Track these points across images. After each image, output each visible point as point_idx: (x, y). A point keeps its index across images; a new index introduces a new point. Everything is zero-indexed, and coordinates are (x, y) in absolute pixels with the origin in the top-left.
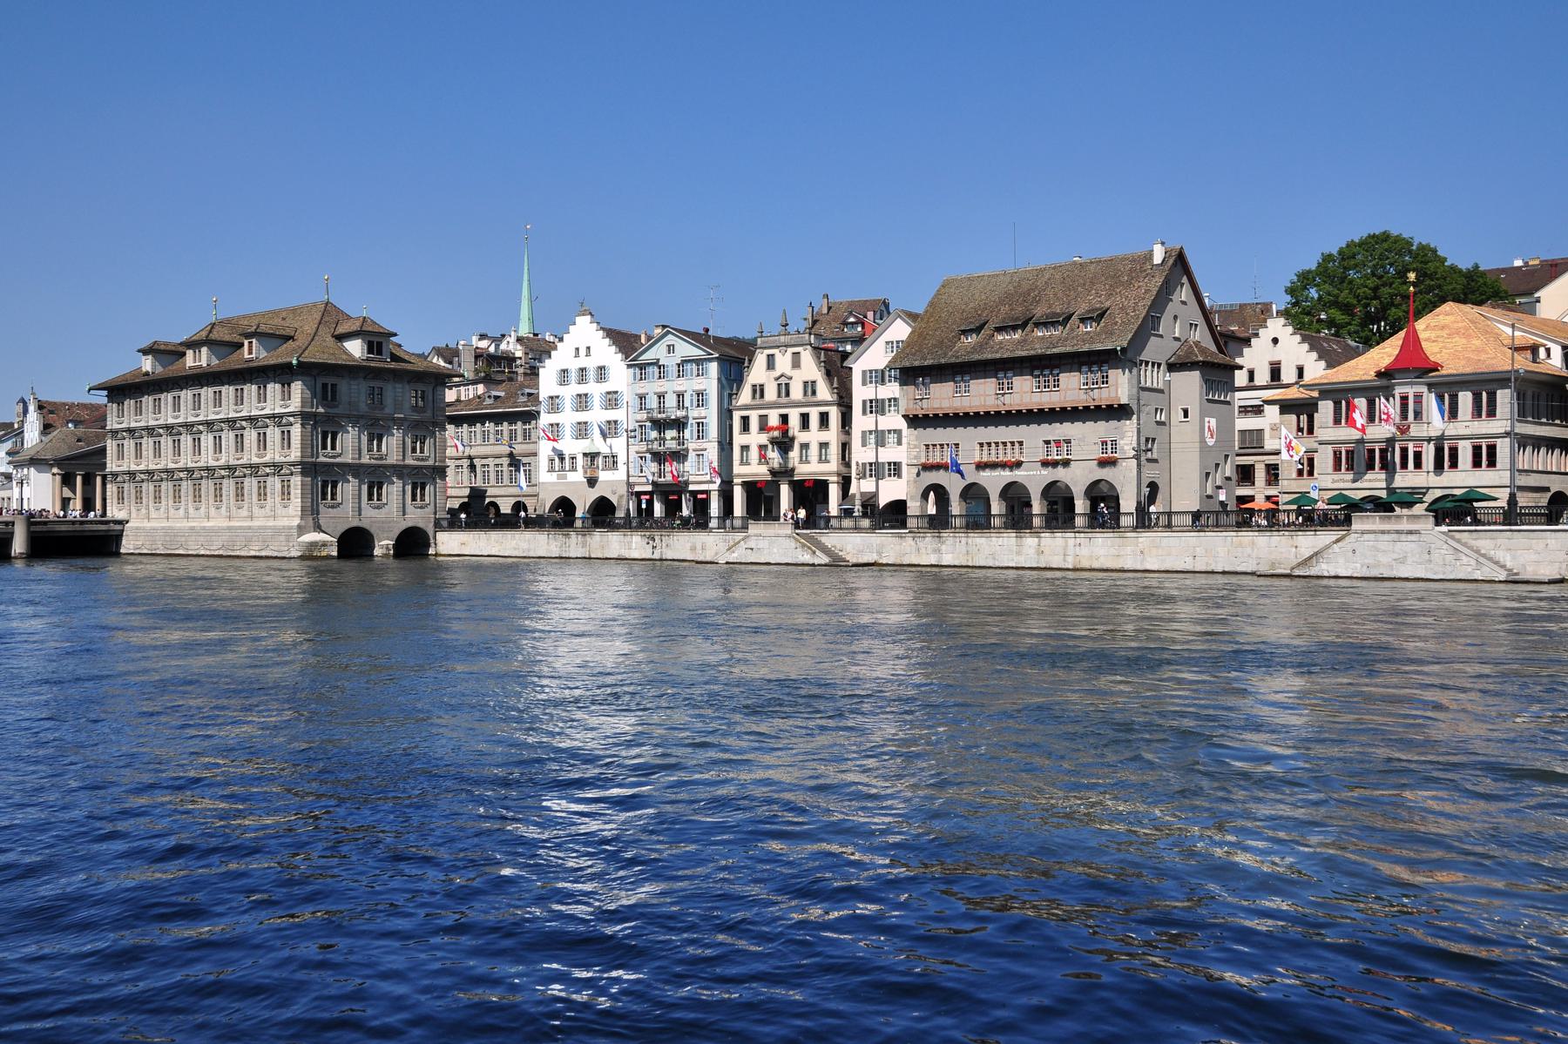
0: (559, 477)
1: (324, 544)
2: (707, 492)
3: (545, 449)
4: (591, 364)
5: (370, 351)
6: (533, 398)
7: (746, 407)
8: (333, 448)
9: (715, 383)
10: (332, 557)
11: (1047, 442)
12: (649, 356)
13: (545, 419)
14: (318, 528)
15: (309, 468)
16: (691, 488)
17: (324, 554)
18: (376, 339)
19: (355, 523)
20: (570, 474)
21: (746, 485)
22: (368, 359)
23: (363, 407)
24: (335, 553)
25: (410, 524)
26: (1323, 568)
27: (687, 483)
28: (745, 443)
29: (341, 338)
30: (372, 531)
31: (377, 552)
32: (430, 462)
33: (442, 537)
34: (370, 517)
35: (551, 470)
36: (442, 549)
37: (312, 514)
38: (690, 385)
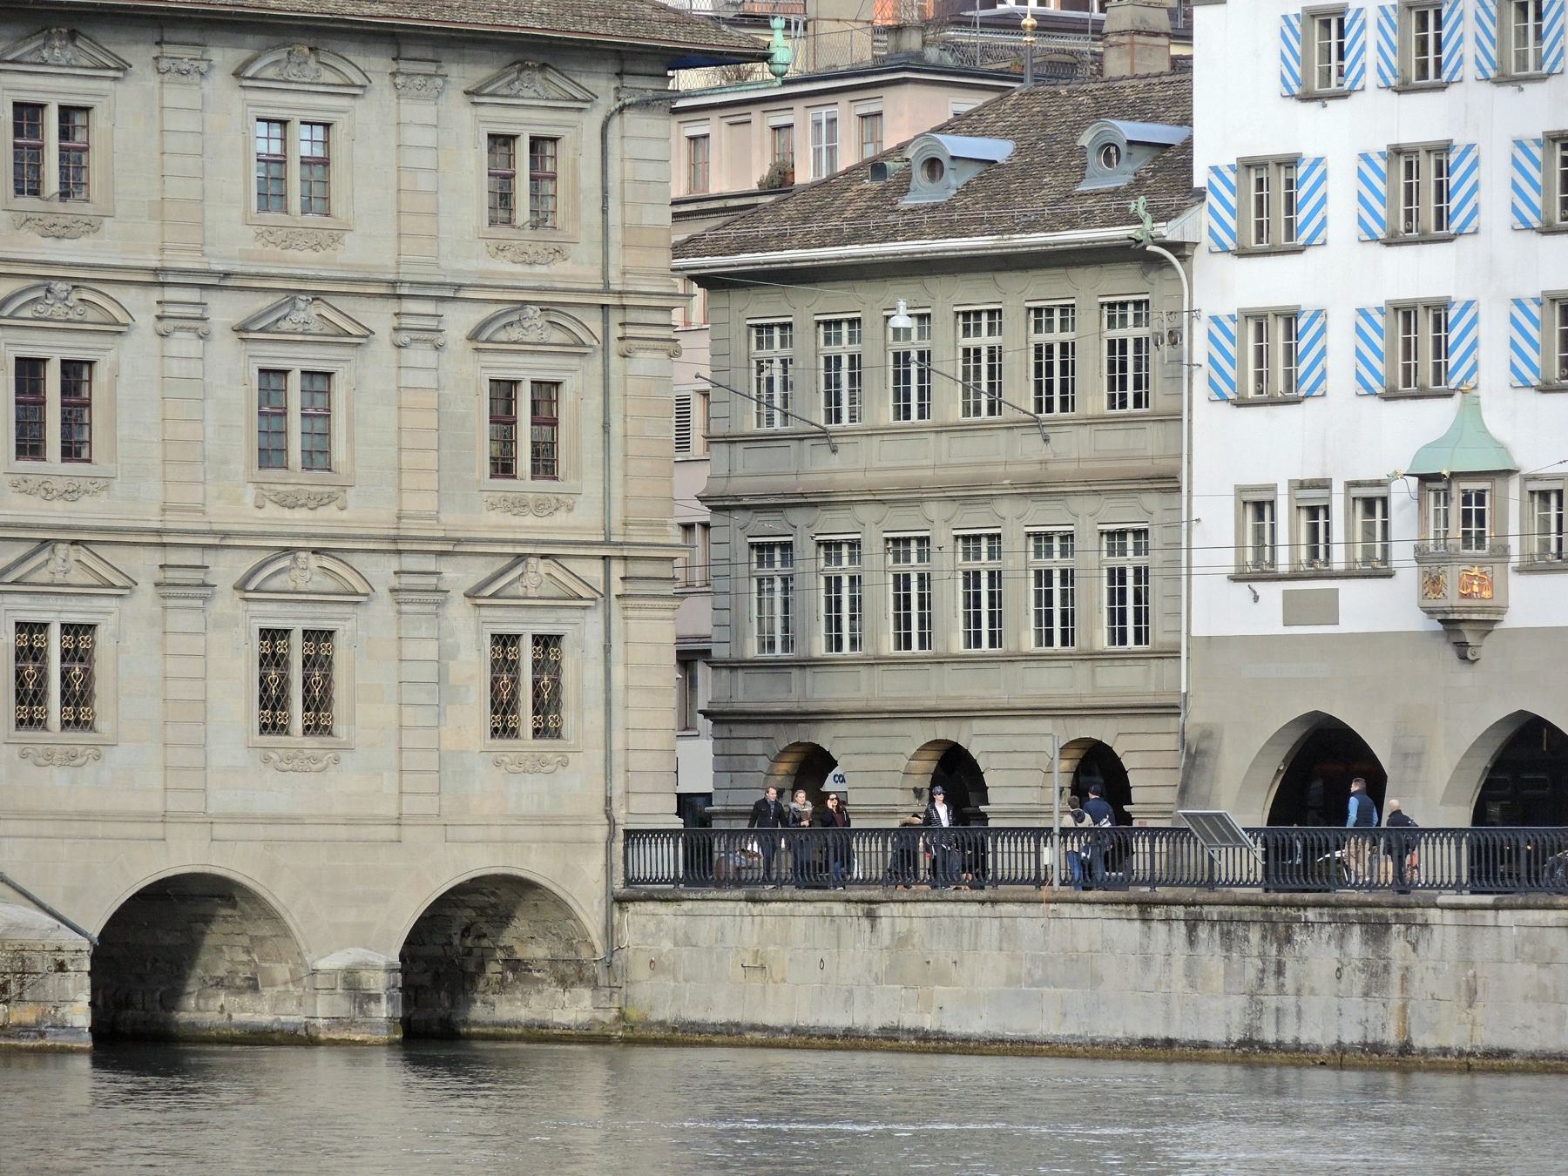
0: (1294, 610)
3: (1231, 450)
6: (1170, 171)
13: (1224, 287)
20: (1349, 591)
23: (232, 234)
33: (651, 928)
35: (1255, 572)
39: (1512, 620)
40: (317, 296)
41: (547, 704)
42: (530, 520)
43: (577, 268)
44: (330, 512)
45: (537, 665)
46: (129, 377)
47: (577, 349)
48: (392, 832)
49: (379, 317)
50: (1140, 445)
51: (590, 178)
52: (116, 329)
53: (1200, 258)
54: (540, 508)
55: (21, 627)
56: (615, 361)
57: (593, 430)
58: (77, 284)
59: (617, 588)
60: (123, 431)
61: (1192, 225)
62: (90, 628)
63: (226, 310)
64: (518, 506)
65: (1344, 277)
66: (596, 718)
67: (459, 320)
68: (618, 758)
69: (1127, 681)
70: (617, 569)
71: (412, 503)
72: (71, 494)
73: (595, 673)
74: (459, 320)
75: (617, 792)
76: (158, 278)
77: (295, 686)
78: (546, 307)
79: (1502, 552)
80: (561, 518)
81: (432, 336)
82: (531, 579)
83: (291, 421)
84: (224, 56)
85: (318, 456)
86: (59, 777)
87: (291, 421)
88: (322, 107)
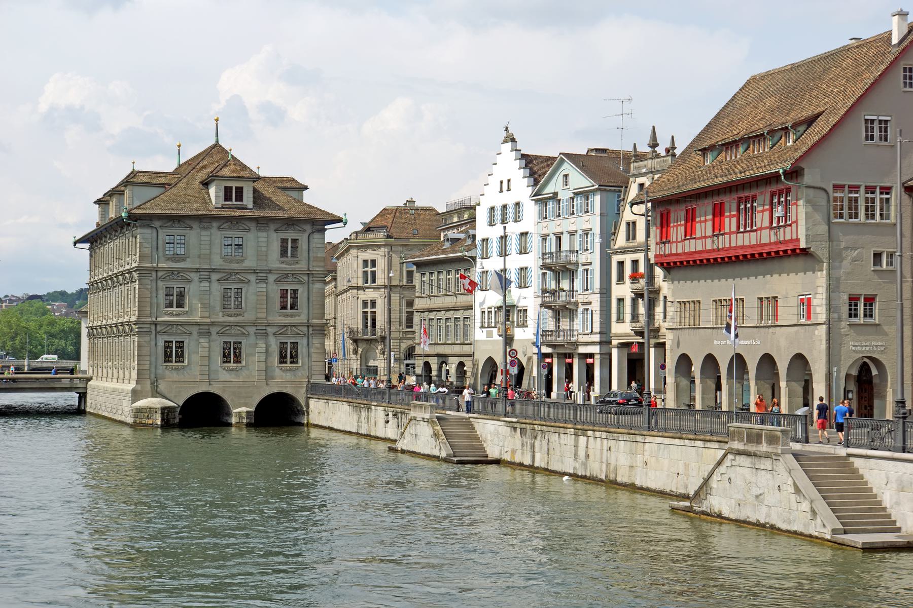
1: (150, 411)
2: (591, 355)
4: (509, 199)
5: (228, 197)
7: (622, 251)
8: (180, 305)
9: (598, 219)
10: (153, 426)
11: (761, 299)
12: (549, 190)
14: (156, 393)
15: (145, 328)
16: (582, 350)
17: (150, 422)
18: (234, 185)
19: (204, 388)
21: (622, 346)
24: (159, 423)
25: (275, 389)
26: (717, 502)
27: (576, 344)
28: (620, 296)
29: (206, 184)
30: (225, 396)
32: (303, 318)
34: (223, 382)
36: (314, 418)
37: (149, 382)
38: (579, 223)
39: (516, 338)
40: (237, 273)
43: (302, 265)
44: (241, 317)
46: (194, 290)
49: (252, 278)
50: (463, 300)
51: (305, 247)
52: (190, 281)
54: (292, 316)
55: (166, 342)
57: (305, 299)
59: (311, 332)
62: (183, 342)
63: (215, 277)
64: (286, 315)
65: (493, 264)
67: (272, 278)
69: (466, 349)
70: (311, 329)
71: (259, 315)
73: (305, 350)
74: (272, 278)
76: (198, 270)
77: (232, 354)
78: (293, 275)
79: (513, 322)
81: (265, 281)
82: (289, 331)
83: (232, 300)
84: (215, 224)
86: (175, 373)
87: (232, 300)
88: (240, 234)
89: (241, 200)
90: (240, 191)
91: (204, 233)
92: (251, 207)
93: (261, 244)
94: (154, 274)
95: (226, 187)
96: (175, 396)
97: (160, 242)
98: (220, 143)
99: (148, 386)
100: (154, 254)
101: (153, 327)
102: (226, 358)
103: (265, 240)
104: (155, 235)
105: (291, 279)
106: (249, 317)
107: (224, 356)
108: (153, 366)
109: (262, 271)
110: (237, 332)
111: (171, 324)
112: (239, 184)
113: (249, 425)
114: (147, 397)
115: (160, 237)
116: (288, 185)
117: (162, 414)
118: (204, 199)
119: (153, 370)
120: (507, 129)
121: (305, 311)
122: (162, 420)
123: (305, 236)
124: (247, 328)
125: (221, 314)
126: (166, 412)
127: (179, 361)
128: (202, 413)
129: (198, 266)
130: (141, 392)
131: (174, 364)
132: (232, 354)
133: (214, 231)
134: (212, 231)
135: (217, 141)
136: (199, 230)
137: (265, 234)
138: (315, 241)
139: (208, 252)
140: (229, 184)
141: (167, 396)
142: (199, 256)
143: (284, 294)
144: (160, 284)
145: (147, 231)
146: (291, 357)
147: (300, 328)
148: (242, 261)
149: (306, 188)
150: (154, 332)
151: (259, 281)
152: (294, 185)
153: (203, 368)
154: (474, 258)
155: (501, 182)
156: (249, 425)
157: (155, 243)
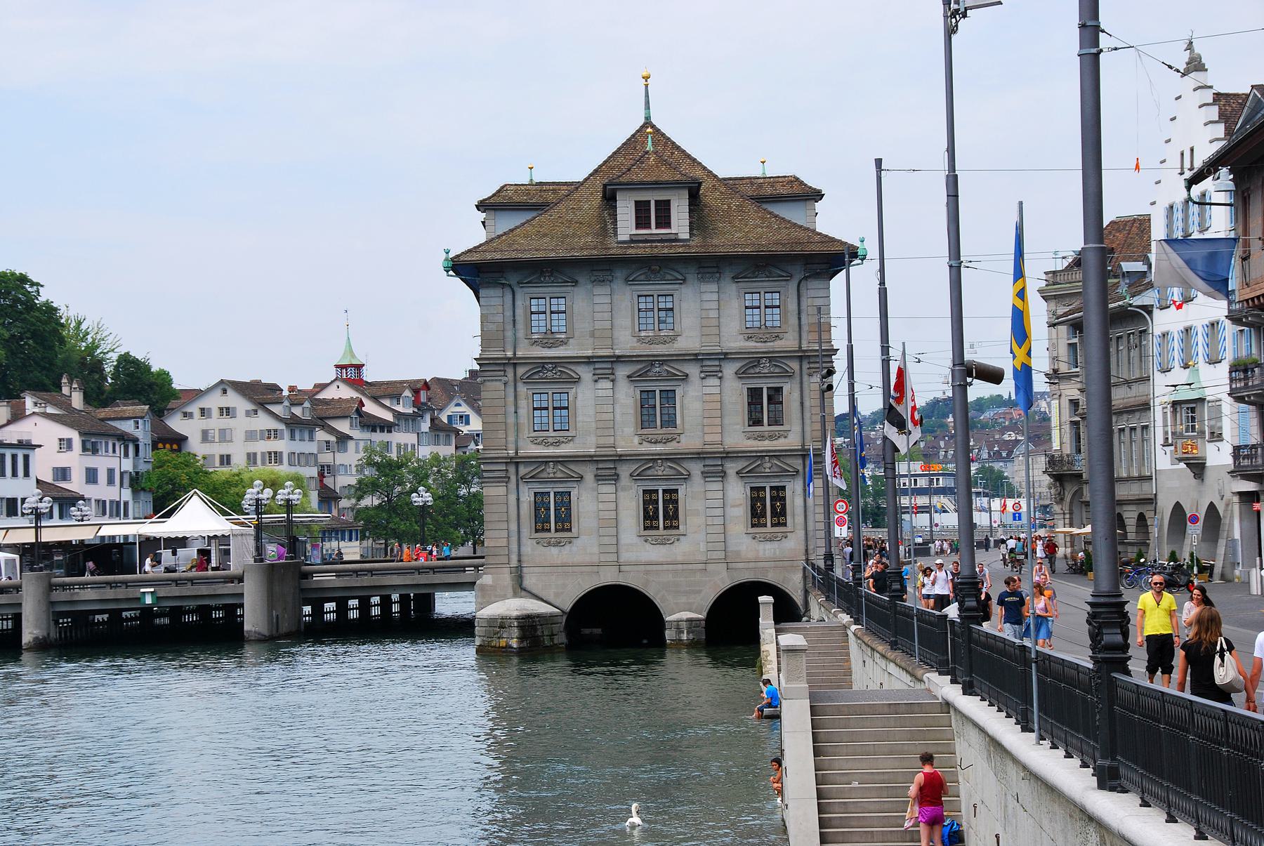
5: (642, 221)
14: (520, 588)
17: (503, 643)
18: (652, 197)
19: (609, 577)
22: (633, 240)
24: (514, 643)
30: (651, 592)
31: (669, 635)
39: (1209, 463)
41: (780, 515)
42: (766, 442)
45: (772, 498)
47: (788, 375)
48: (701, 566)
52: (577, 381)
53: (1156, 312)
54: (771, 437)
56: (805, 378)
58: (556, 365)
60: (580, 418)
61: (1148, 298)
64: (761, 437)
66: (800, 519)
68: (810, 534)
72: (557, 444)
73: (799, 501)
75: (811, 547)
80: (782, 440)
81: (718, 374)
85: (670, 421)
86: (554, 551)
88: (666, 288)
89: (668, 225)
90: (664, 209)
91: (599, 290)
92: (687, 236)
93: (706, 306)
94: (510, 372)
95: (637, 203)
96: (557, 595)
97: (519, 311)
98: (654, 121)
99: (506, 578)
100: (509, 334)
101: (512, 469)
102: (649, 519)
103: (715, 297)
104: (509, 297)
105: (766, 368)
106: (690, 441)
107: (647, 516)
108: (514, 539)
109: (710, 356)
110: (668, 471)
111: (544, 461)
112: (662, 196)
113: (692, 645)
114: (504, 597)
115: (519, 303)
116: (784, 191)
117: (521, 627)
118: (604, 229)
119: (514, 547)
120: (1190, 46)
121: (796, 428)
122: (521, 639)
123: (792, 286)
124: (686, 464)
125: (636, 440)
126: (528, 624)
127: (563, 530)
128: (612, 626)
129: (589, 353)
130: (493, 587)
131: (553, 534)
132: (661, 513)
133: (618, 285)
134: (615, 286)
135: (648, 118)
136: (589, 286)
137: (714, 287)
138: (812, 293)
139: (608, 325)
140: (643, 196)
141: (540, 595)
142: (592, 335)
143: (754, 394)
144: (522, 389)
145: (497, 292)
146: (774, 513)
147: (789, 461)
148: (673, 339)
149: (817, 195)
150: (513, 478)
151: (706, 375)
152: (796, 190)
153: (606, 540)
154: (1148, 309)
155: (1182, 154)
156: (692, 645)
157: (509, 313)
